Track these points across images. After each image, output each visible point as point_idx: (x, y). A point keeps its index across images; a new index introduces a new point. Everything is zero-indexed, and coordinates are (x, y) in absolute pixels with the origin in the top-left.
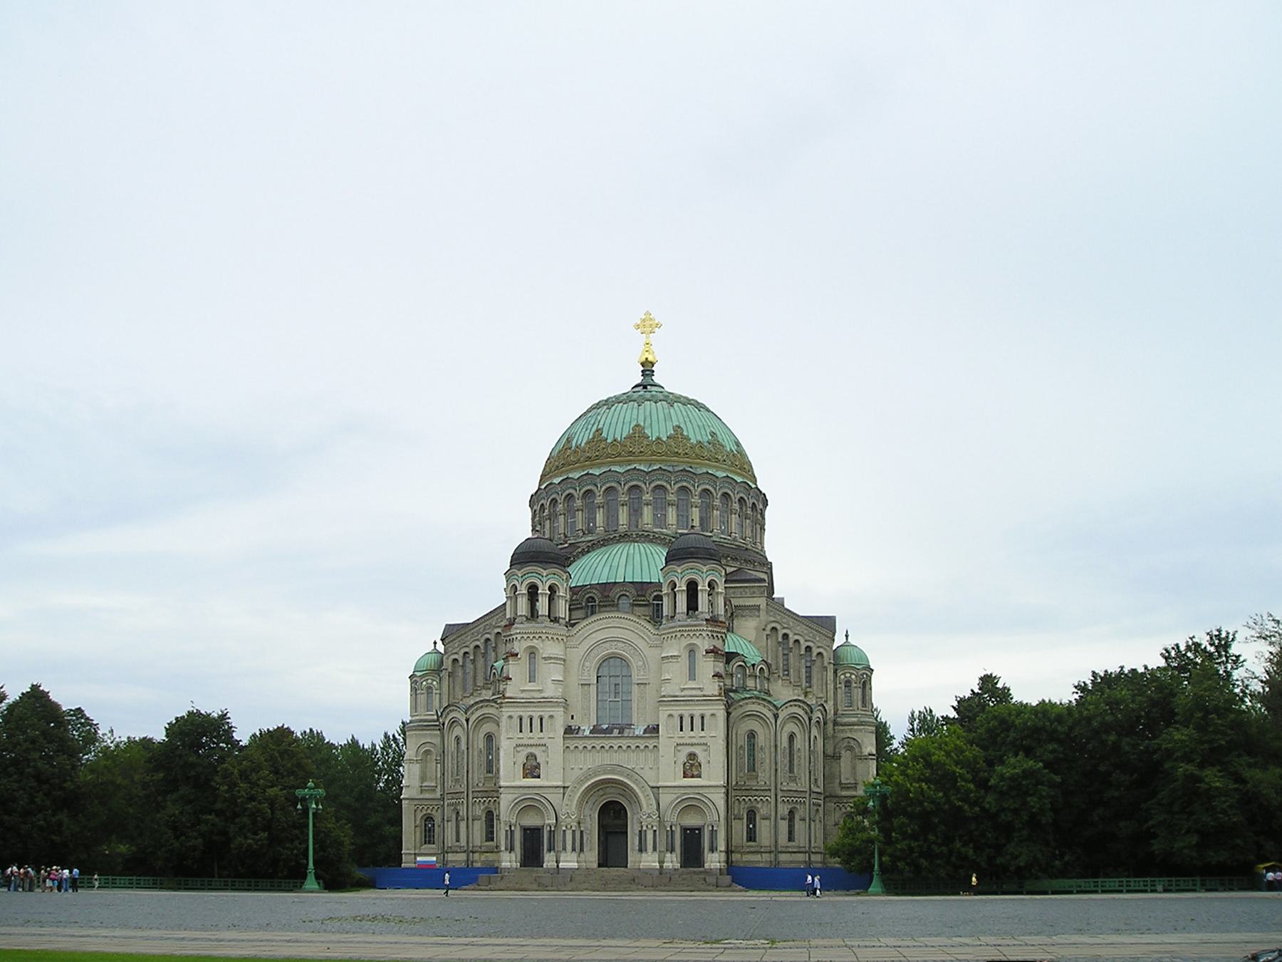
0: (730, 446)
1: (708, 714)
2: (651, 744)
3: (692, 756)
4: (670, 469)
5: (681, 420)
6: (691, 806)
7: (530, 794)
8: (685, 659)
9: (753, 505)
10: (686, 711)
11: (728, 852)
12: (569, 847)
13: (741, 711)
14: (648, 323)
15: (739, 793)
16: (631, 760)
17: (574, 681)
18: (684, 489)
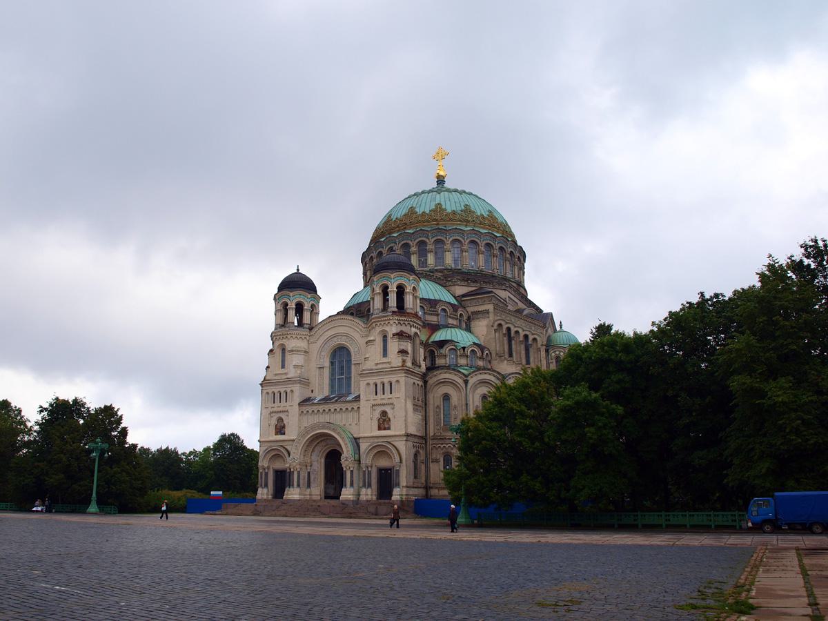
0: (480, 211)
1: (393, 380)
2: (355, 405)
3: (384, 413)
4: (429, 229)
5: (443, 200)
6: (381, 451)
7: (275, 446)
8: (379, 340)
9: (518, 257)
10: (378, 380)
11: (427, 488)
12: (295, 484)
13: (435, 379)
14: (440, 155)
15: (435, 441)
16: (338, 419)
17: (314, 365)
18: (438, 241)
